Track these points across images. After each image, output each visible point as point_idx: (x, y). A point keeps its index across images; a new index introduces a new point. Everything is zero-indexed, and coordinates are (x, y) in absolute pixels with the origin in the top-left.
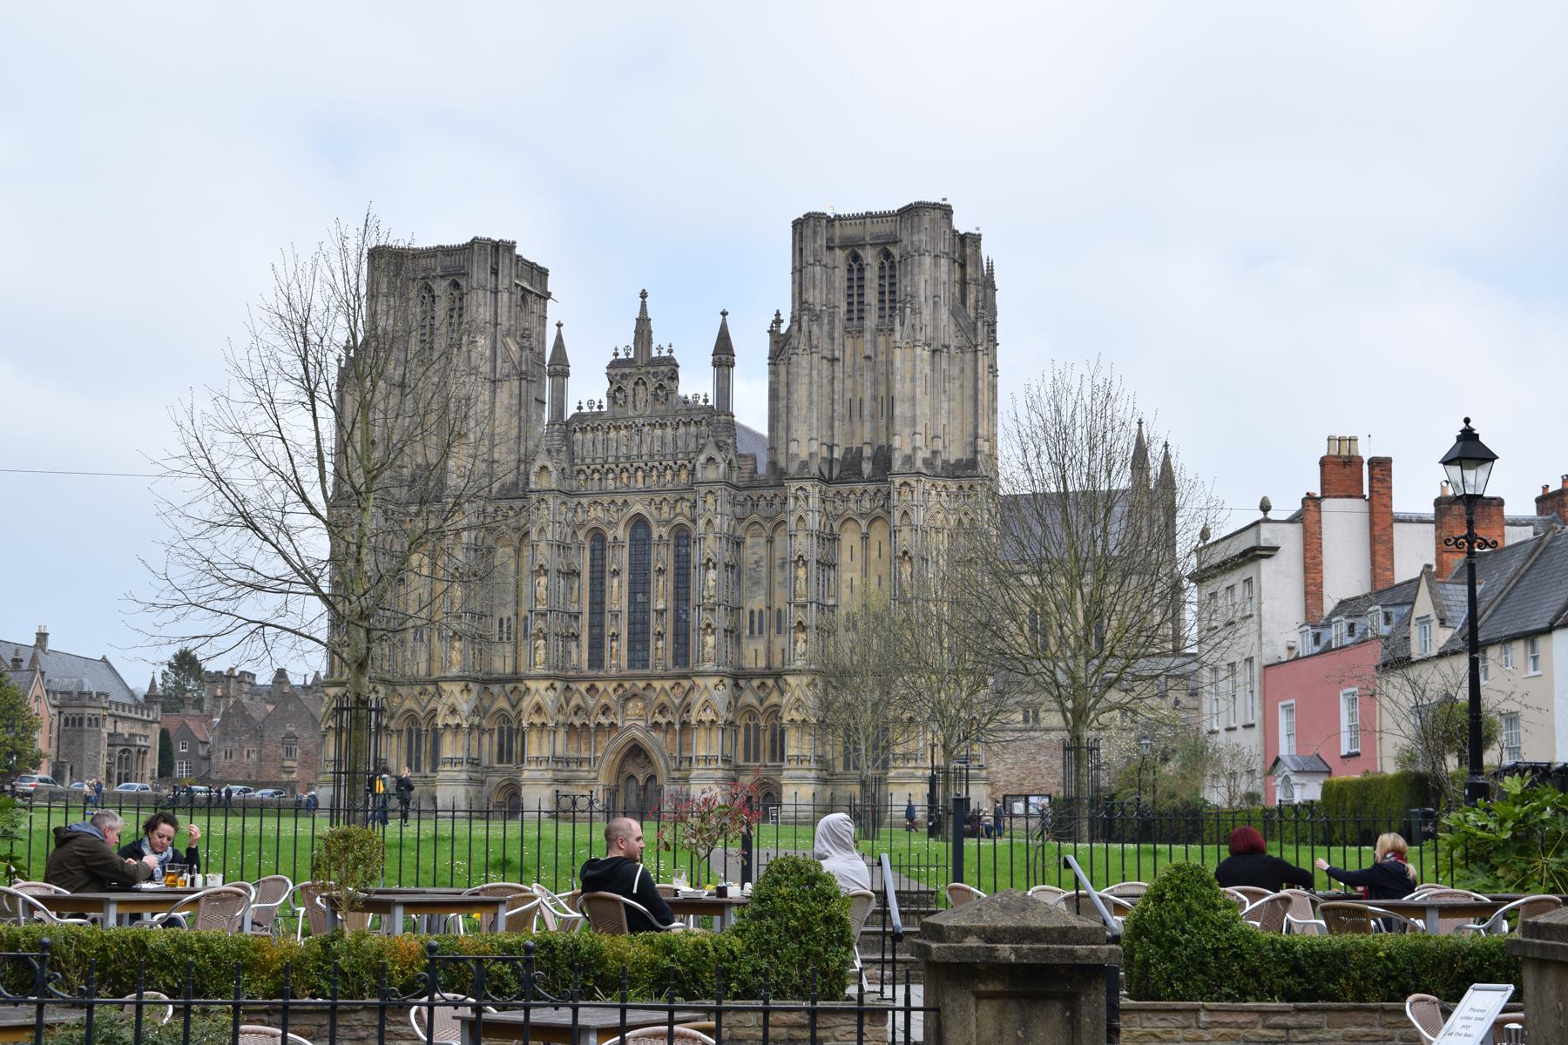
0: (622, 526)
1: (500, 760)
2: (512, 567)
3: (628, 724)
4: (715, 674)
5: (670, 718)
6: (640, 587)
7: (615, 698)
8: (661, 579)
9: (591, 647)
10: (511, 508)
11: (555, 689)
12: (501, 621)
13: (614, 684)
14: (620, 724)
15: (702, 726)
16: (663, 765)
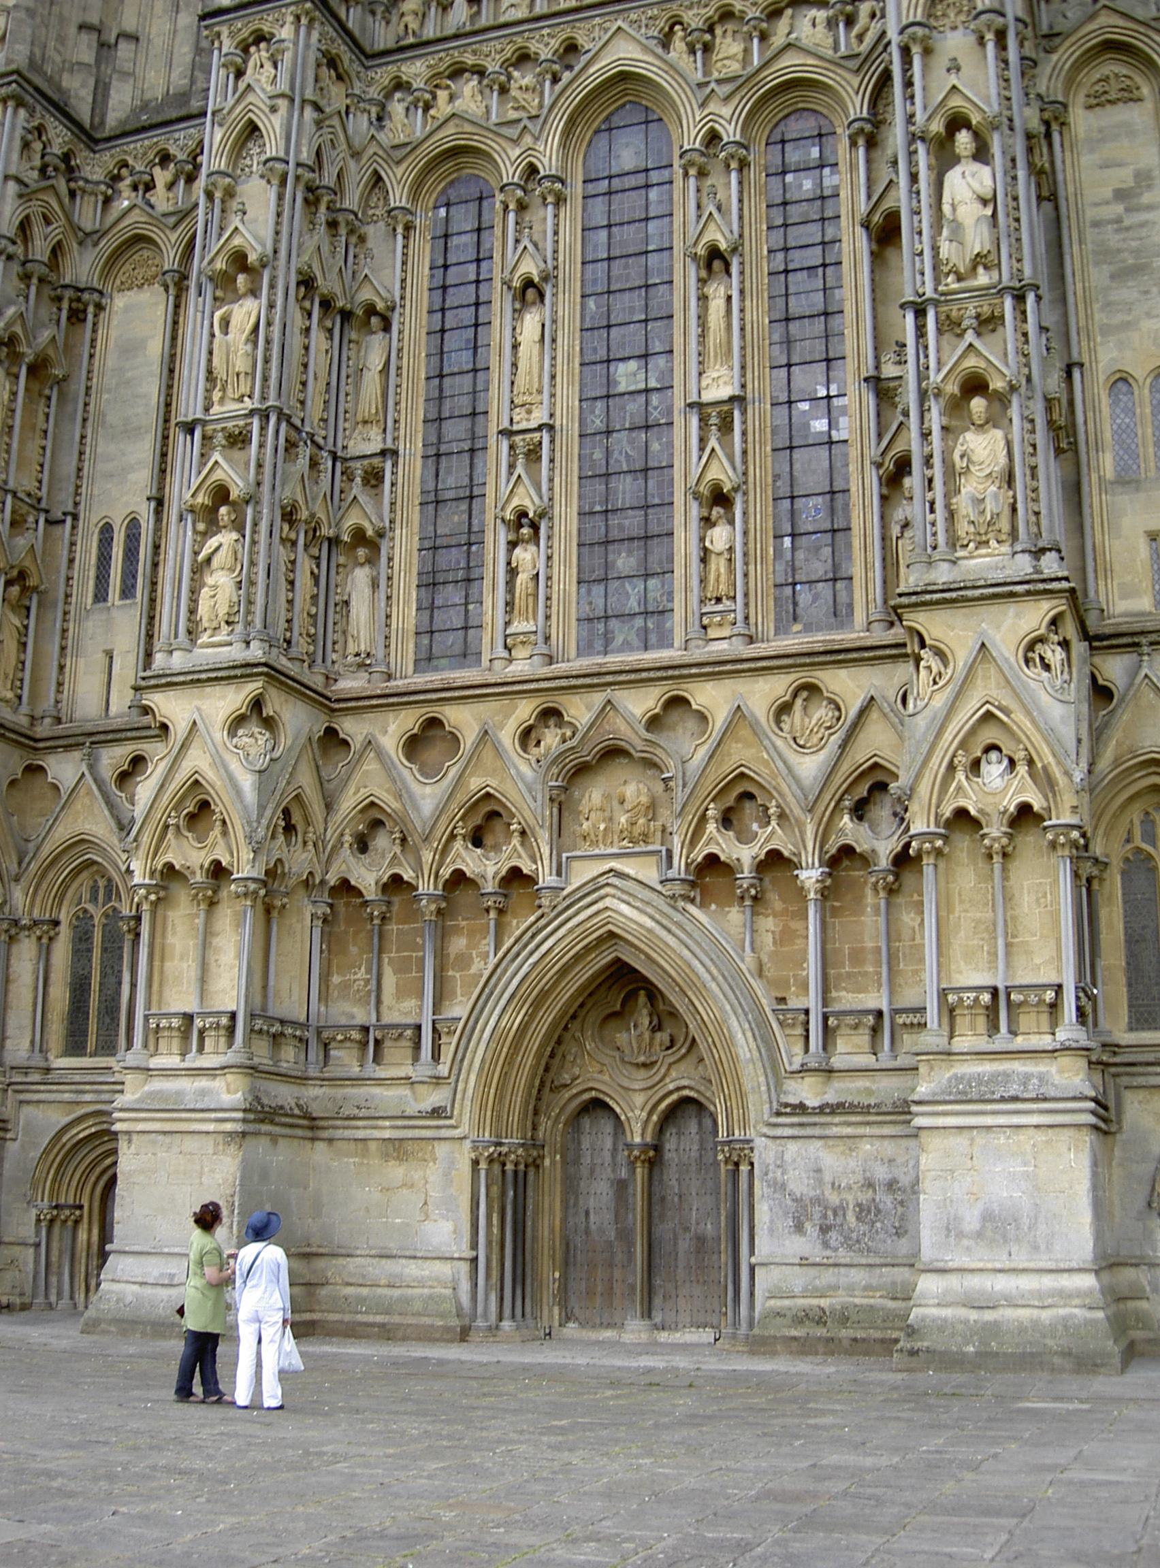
0: (558, 125)
1: (75, 1045)
2: (156, 347)
3: (582, 874)
4: (1035, 588)
5: (770, 837)
6: (629, 338)
7: (524, 767)
8: (717, 292)
9: (430, 582)
10: (165, 159)
11: (269, 723)
12: (107, 531)
13: (525, 710)
14: (546, 878)
15: (963, 842)
16: (745, 1046)
